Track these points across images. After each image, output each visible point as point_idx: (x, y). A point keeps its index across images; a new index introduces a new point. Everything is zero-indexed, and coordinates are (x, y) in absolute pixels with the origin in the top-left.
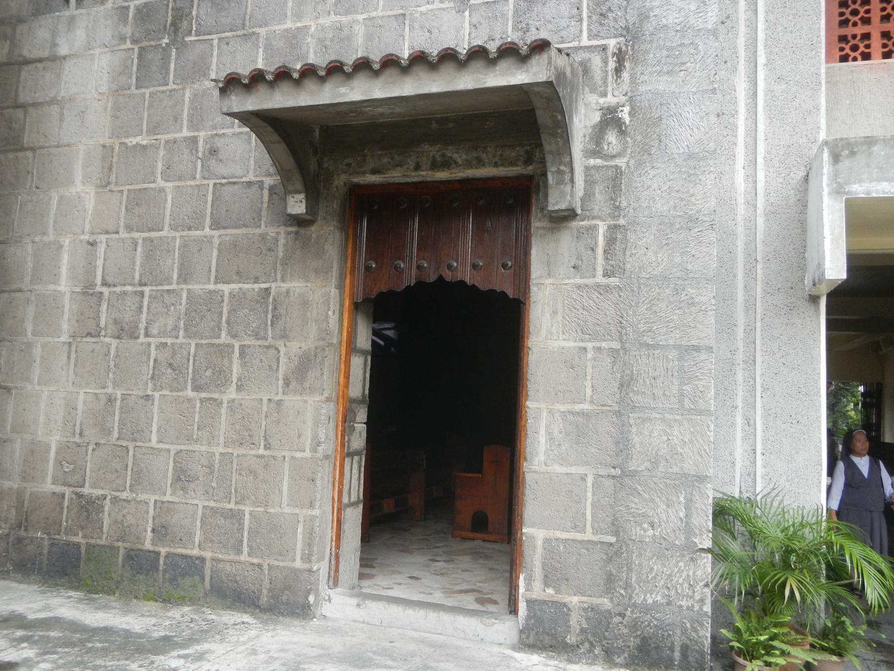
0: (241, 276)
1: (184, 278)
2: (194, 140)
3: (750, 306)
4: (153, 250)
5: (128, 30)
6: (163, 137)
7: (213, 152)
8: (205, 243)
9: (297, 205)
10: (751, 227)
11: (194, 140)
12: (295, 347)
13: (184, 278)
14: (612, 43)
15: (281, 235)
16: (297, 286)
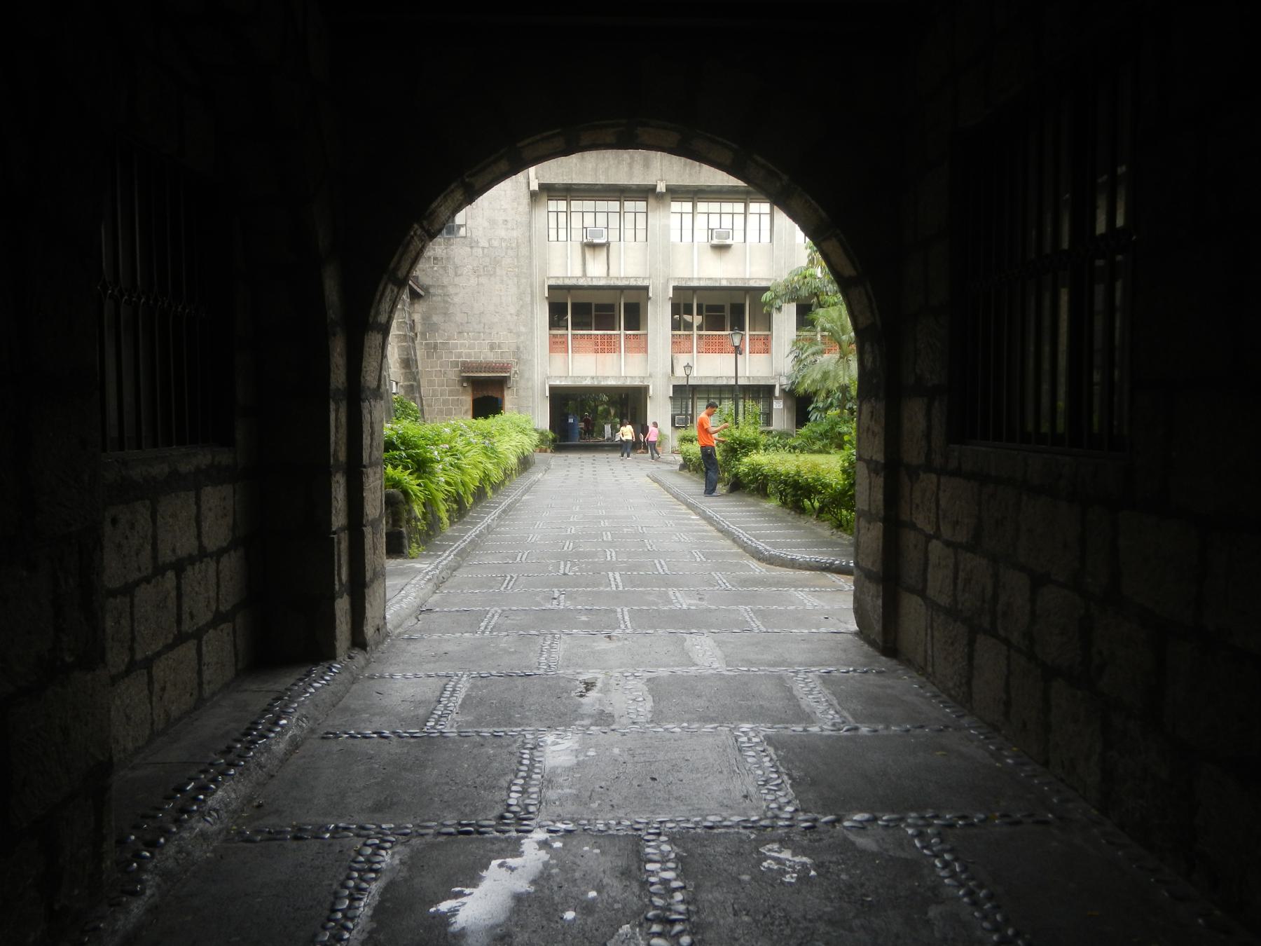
0: (453, 396)
1: (441, 396)
2: (441, 371)
3: (538, 398)
4: (433, 390)
5: (423, 347)
6: (434, 369)
7: (445, 373)
8: (445, 390)
9: (465, 385)
10: (538, 385)
11: (441, 371)
12: (465, 408)
13: (441, 396)
14: (516, 360)
15: (461, 389)
16: (464, 397)
